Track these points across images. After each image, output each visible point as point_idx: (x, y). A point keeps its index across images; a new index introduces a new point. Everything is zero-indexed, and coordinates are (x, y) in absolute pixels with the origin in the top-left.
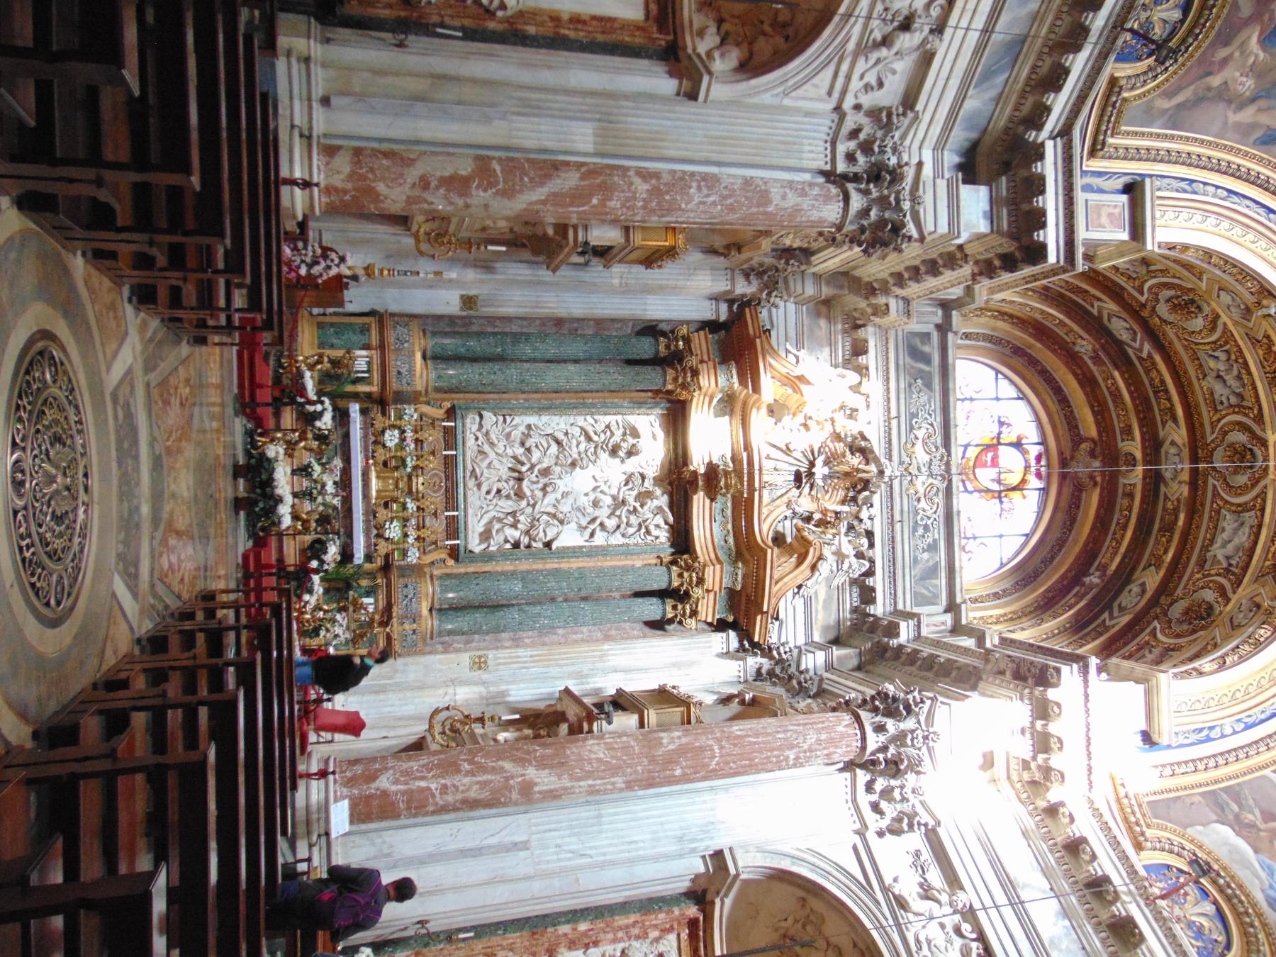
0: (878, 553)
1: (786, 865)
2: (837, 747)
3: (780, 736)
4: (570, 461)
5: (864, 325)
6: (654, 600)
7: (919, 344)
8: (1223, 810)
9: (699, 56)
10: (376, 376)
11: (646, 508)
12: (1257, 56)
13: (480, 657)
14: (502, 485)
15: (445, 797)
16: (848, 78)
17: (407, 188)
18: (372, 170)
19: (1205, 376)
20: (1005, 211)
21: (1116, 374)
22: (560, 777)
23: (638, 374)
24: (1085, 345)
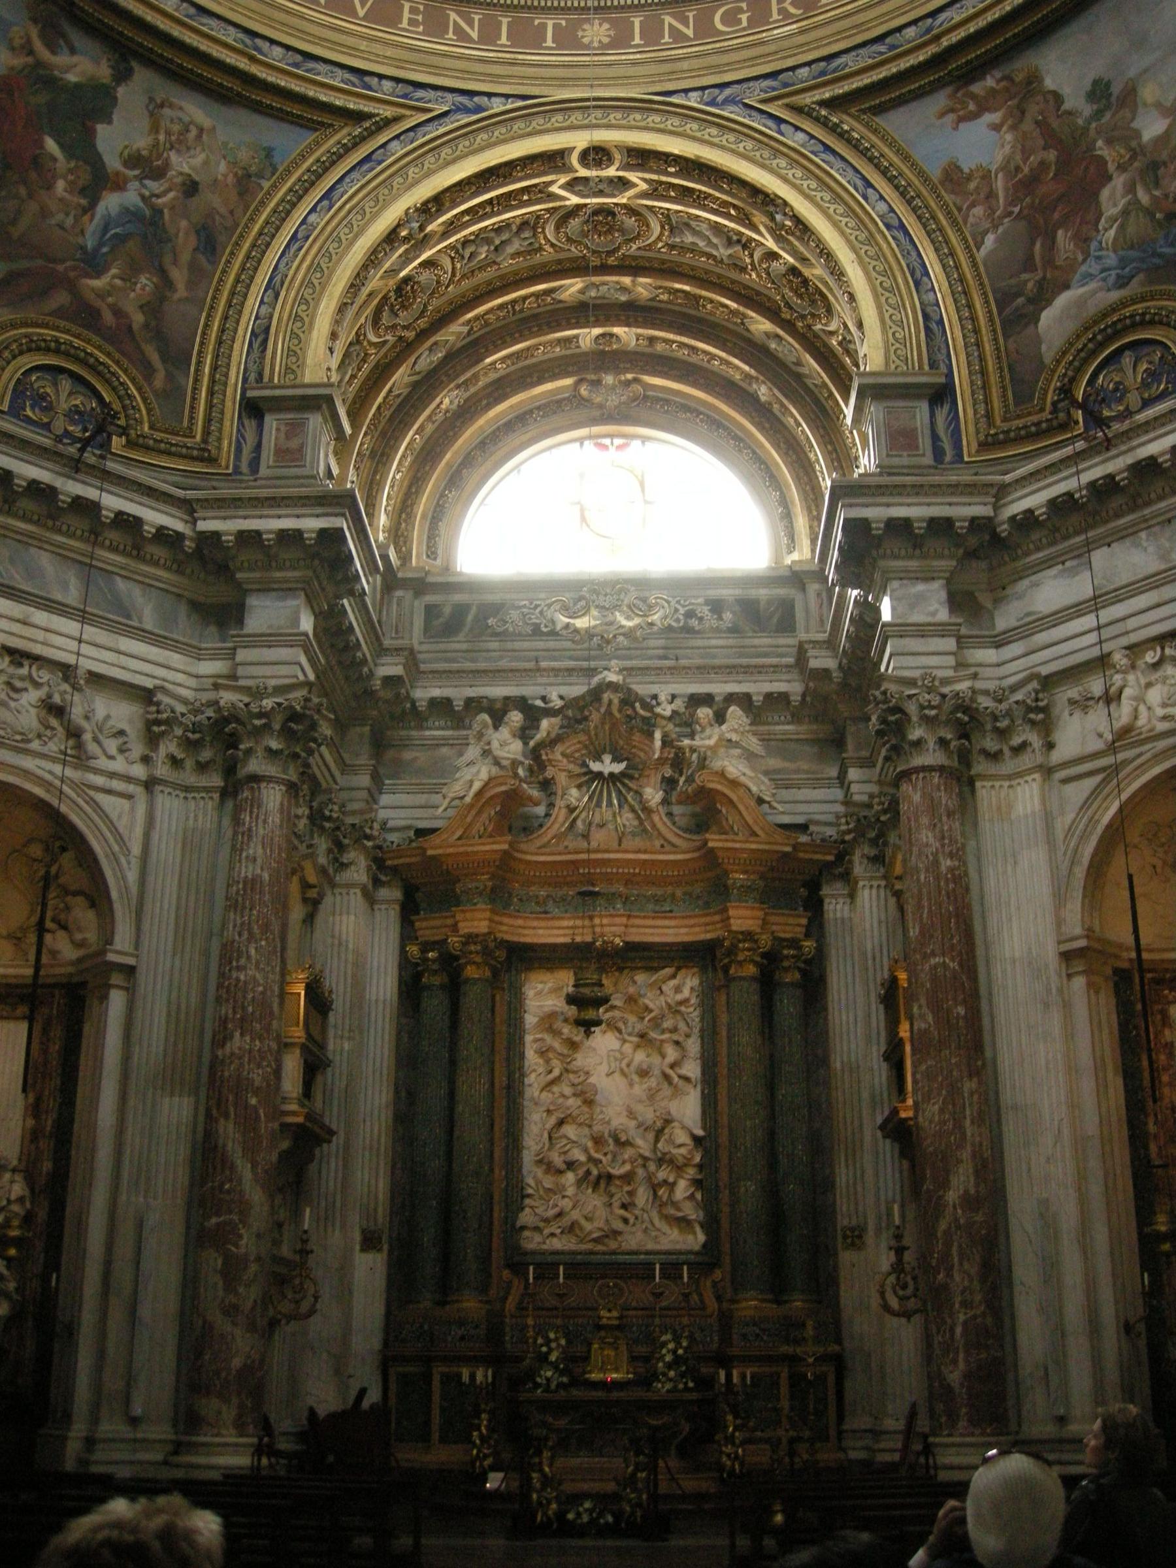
0: (720, 688)
1: (1080, 872)
3: (922, 877)
4: (585, 1109)
5: (413, 703)
7: (441, 620)
8: (1022, 316)
9: (80, 960)
11: (651, 1006)
12: (114, 277)
13: (845, 1237)
14: (616, 1204)
16: (112, 775)
19: (494, 262)
20: (278, 574)
21: (488, 360)
22: (961, 1161)
24: (447, 400)
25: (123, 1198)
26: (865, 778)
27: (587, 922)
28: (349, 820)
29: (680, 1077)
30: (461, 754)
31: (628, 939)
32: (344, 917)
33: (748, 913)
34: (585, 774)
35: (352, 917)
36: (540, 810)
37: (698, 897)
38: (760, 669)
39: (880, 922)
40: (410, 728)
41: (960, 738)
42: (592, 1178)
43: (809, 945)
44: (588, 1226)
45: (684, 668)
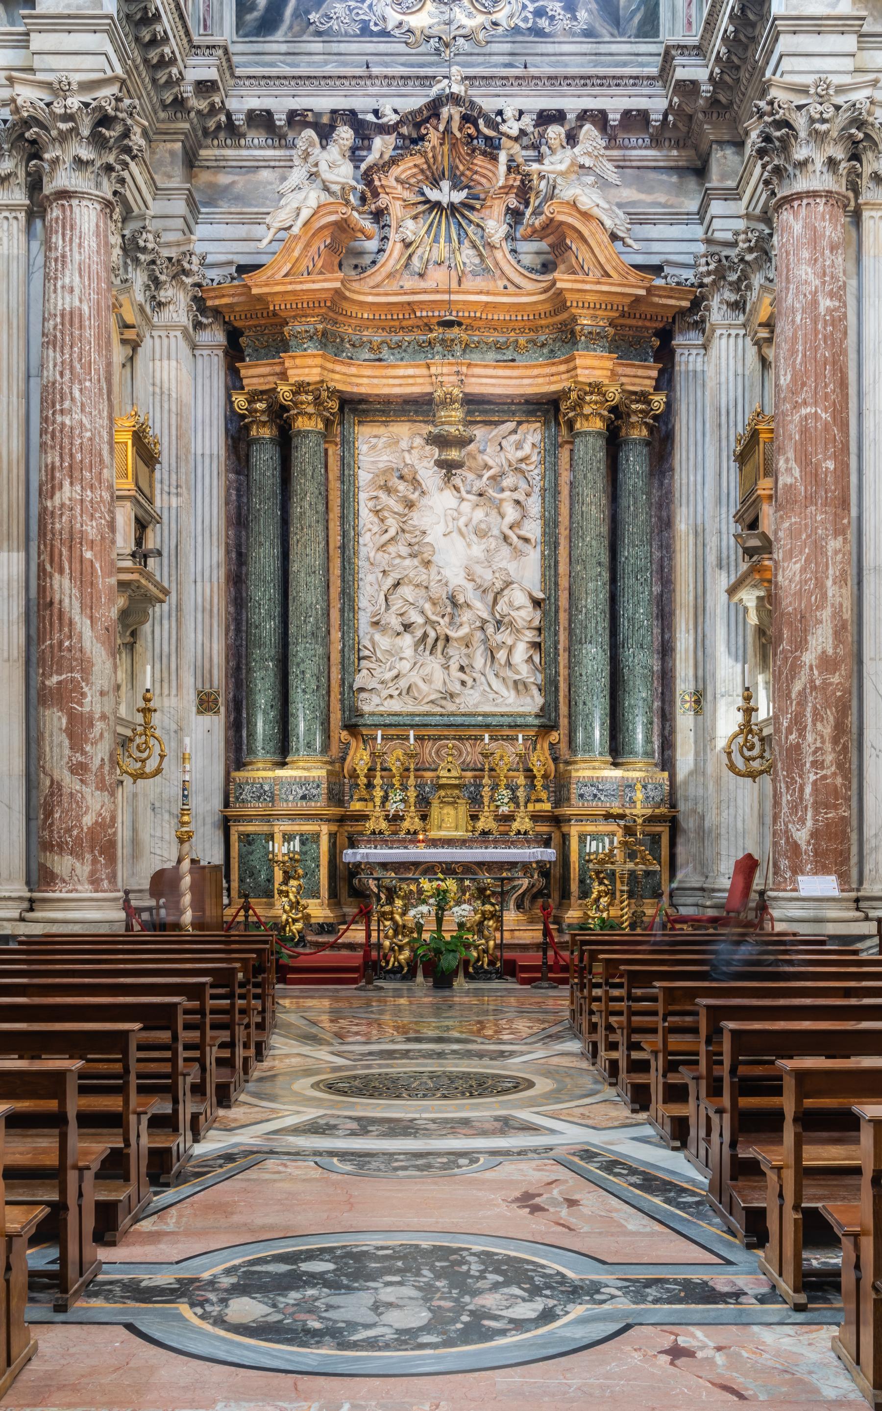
3: (798, 319)
5: (229, 115)
7: (256, 14)
10: (309, 827)
11: (491, 463)
14: (454, 666)
15: (827, 763)
17: (87, 790)
23: (303, 473)
27: (424, 371)
28: (165, 253)
29: (519, 537)
30: (284, 179)
31: (467, 390)
33: (596, 363)
35: (173, 363)
36: (372, 245)
37: (543, 345)
38: (617, 80)
39: (736, 375)
41: (849, 160)
42: (430, 641)
43: (659, 400)
45: (533, 78)
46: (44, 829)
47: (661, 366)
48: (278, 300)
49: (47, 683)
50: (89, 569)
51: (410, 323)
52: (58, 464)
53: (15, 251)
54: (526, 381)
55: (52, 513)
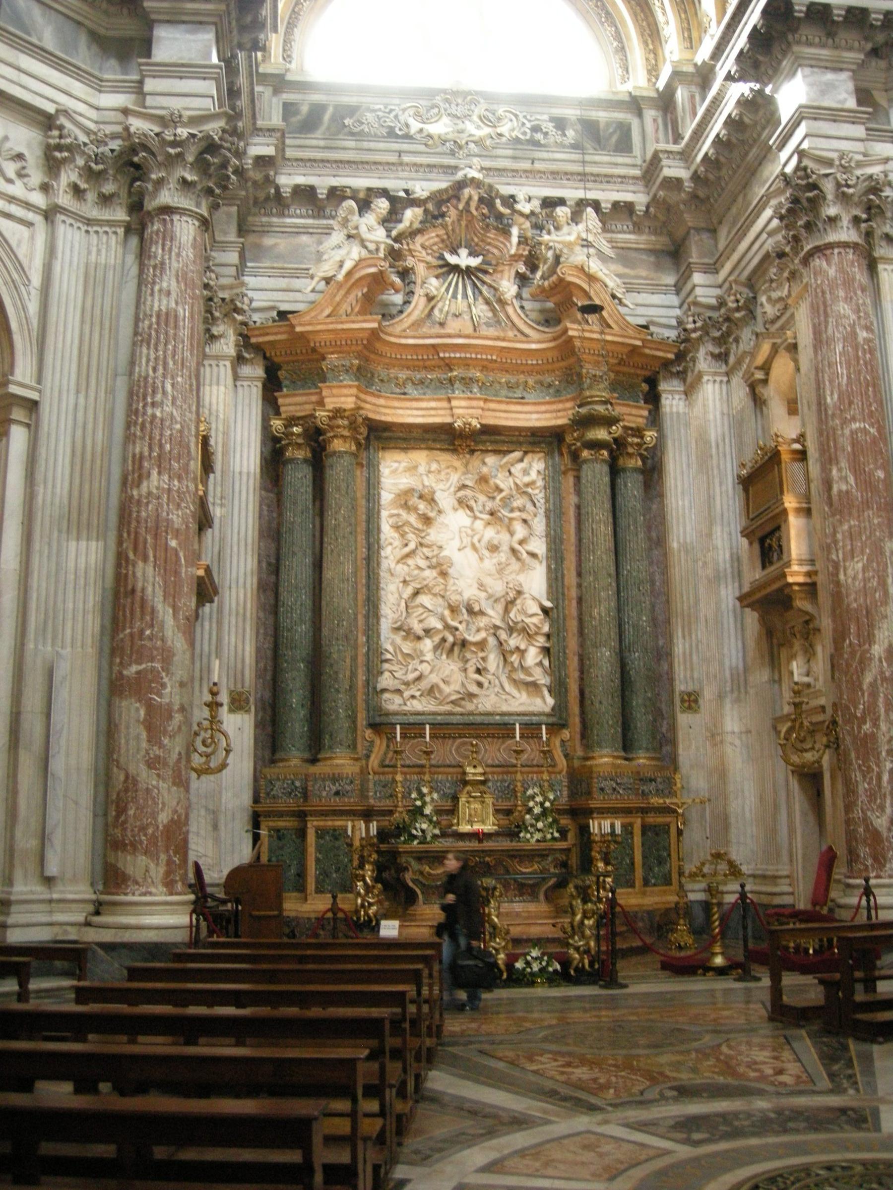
0: (573, 193)
2: (854, 279)
5: (277, 188)
6: (619, 480)
7: (299, 117)
11: (502, 486)
13: (683, 701)
14: (471, 669)
18: (143, 829)
23: (338, 489)
25: (31, 646)
26: (708, 283)
27: (445, 404)
28: (221, 295)
30: (320, 243)
31: (484, 422)
32: (215, 388)
34: (441, 267)
35: (222, 388)
36: (398, 299)
37: (550, 386)
38: (608, 179)
39: (723, 414)
40: (271, 215)
42: (447, 645)
44: (447, 689)
45: (540, 172)
46: (115, 826)
47: (651, 407)
48: (318, 338)
49: (125, 672)
50: (174, 558)
51: (433, 363)
52: (146, 454)
53: (112, 262)
54: (534, 416)
55: (139, 502)
